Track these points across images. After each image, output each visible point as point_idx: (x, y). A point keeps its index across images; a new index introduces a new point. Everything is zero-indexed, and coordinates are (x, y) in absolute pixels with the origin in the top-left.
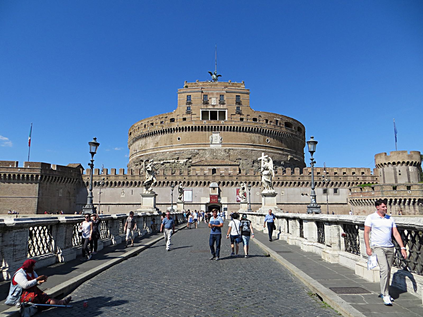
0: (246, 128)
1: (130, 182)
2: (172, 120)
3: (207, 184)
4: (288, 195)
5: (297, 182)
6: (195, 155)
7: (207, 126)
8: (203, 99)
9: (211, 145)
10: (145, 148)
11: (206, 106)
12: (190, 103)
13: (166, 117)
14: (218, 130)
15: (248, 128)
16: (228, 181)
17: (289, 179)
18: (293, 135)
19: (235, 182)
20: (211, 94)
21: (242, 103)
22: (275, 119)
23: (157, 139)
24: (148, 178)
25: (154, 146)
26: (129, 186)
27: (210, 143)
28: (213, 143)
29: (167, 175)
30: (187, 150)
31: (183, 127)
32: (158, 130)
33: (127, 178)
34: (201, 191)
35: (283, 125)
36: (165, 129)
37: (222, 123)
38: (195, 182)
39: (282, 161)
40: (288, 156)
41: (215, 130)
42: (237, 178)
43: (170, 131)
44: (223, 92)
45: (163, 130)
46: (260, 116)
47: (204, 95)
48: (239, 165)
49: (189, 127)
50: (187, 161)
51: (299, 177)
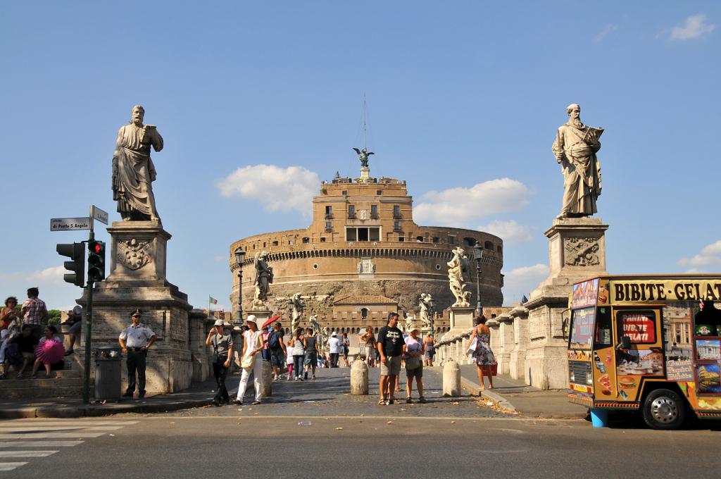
0: (408, 251)
2: (306, 240)
3: (356, 331)
6: (338, 289)
7: (354, 250)
8: (348, 212)
31: (321, 251)
41: (365, 255)
43: (303, 255)
45: (293, 253)
46: (426, 233)
48: (396, 304)
49: (330, 251)
50: (327, 298)
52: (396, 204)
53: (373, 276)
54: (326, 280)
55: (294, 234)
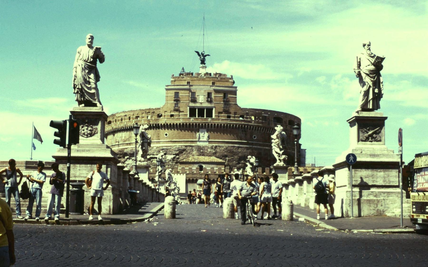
3: (195, 181)
8: (190, 96)
10: (129, 140)
13: (154, 112)
22: (263, 115)
28: (200, 140)
31: (170, 124)
46: (247, 113)
48: (224, 163)
49: (177, 124)
50: (174, 158)
55: (151, 111)
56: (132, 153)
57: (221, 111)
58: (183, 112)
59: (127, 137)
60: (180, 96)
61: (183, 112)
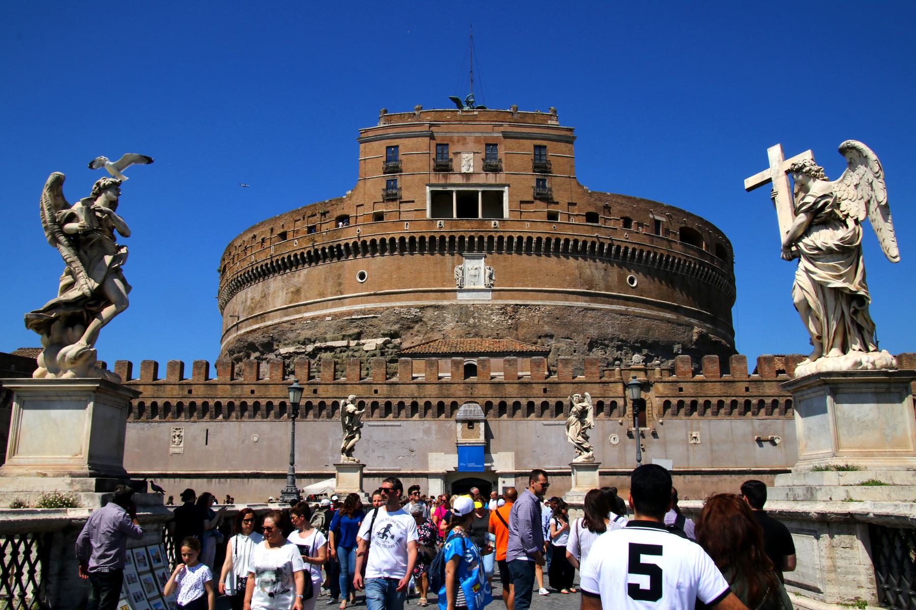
0: (567, 241)
1: (199, 402)
3: (448, 409)
4: (711, 444)
5: (741, 400)
6: (409, 323)
9: (461, 296)
10: (261, 307)
11: (445, 177)
12: (396, 170)
14: (481, 249)
15: (571, 243)
16: (515, 400)
17: (715, 391)
18: (704, 268)
19: (538, 402)
20: (458, 141)
21: (554, 168)
23: (296, 279)
24: (69, 286)
25: (288, 300)
26: (199, 418)
27: (457, 288)
28: (466, 287)
29: (318, 380)
30: (388, 308)
32: (299, 253)
33: (190, 392)
34: (427, 432)
35: (675, 234)
36: (321, 247)
37: (493, 226)
38: (408, 402)
39: (674, 343)
40: (693, 328)
41: (471, 249)
42: (545, 390)
43: (337, 253)
44: (496, 135)
45: (316, 251)
47: (437, 145)
48: (546, 354)
49: (392, 240)
50: (385, 343)
51: (746, 384)
52: (538, 142)
53: (490, 294)
54: (384, 305)
56: (266, 340)
57: (531, 199)
58: (413, 202)
59: (258, 299)
60: (400, 157)
61: (413, 202)
